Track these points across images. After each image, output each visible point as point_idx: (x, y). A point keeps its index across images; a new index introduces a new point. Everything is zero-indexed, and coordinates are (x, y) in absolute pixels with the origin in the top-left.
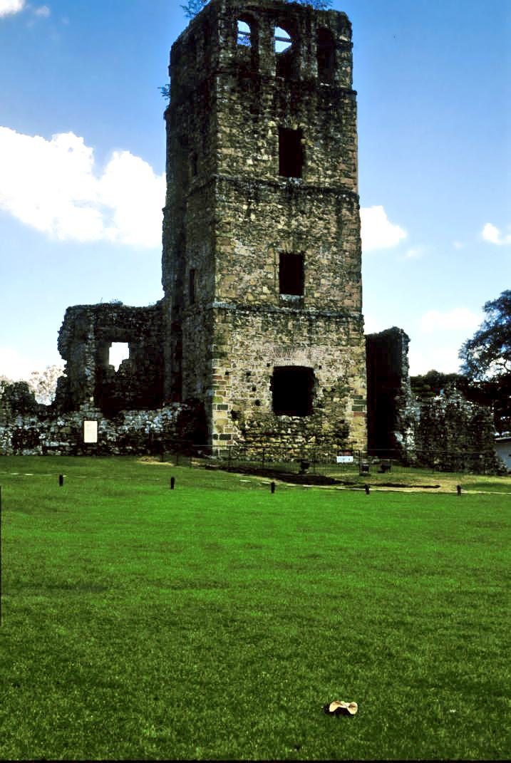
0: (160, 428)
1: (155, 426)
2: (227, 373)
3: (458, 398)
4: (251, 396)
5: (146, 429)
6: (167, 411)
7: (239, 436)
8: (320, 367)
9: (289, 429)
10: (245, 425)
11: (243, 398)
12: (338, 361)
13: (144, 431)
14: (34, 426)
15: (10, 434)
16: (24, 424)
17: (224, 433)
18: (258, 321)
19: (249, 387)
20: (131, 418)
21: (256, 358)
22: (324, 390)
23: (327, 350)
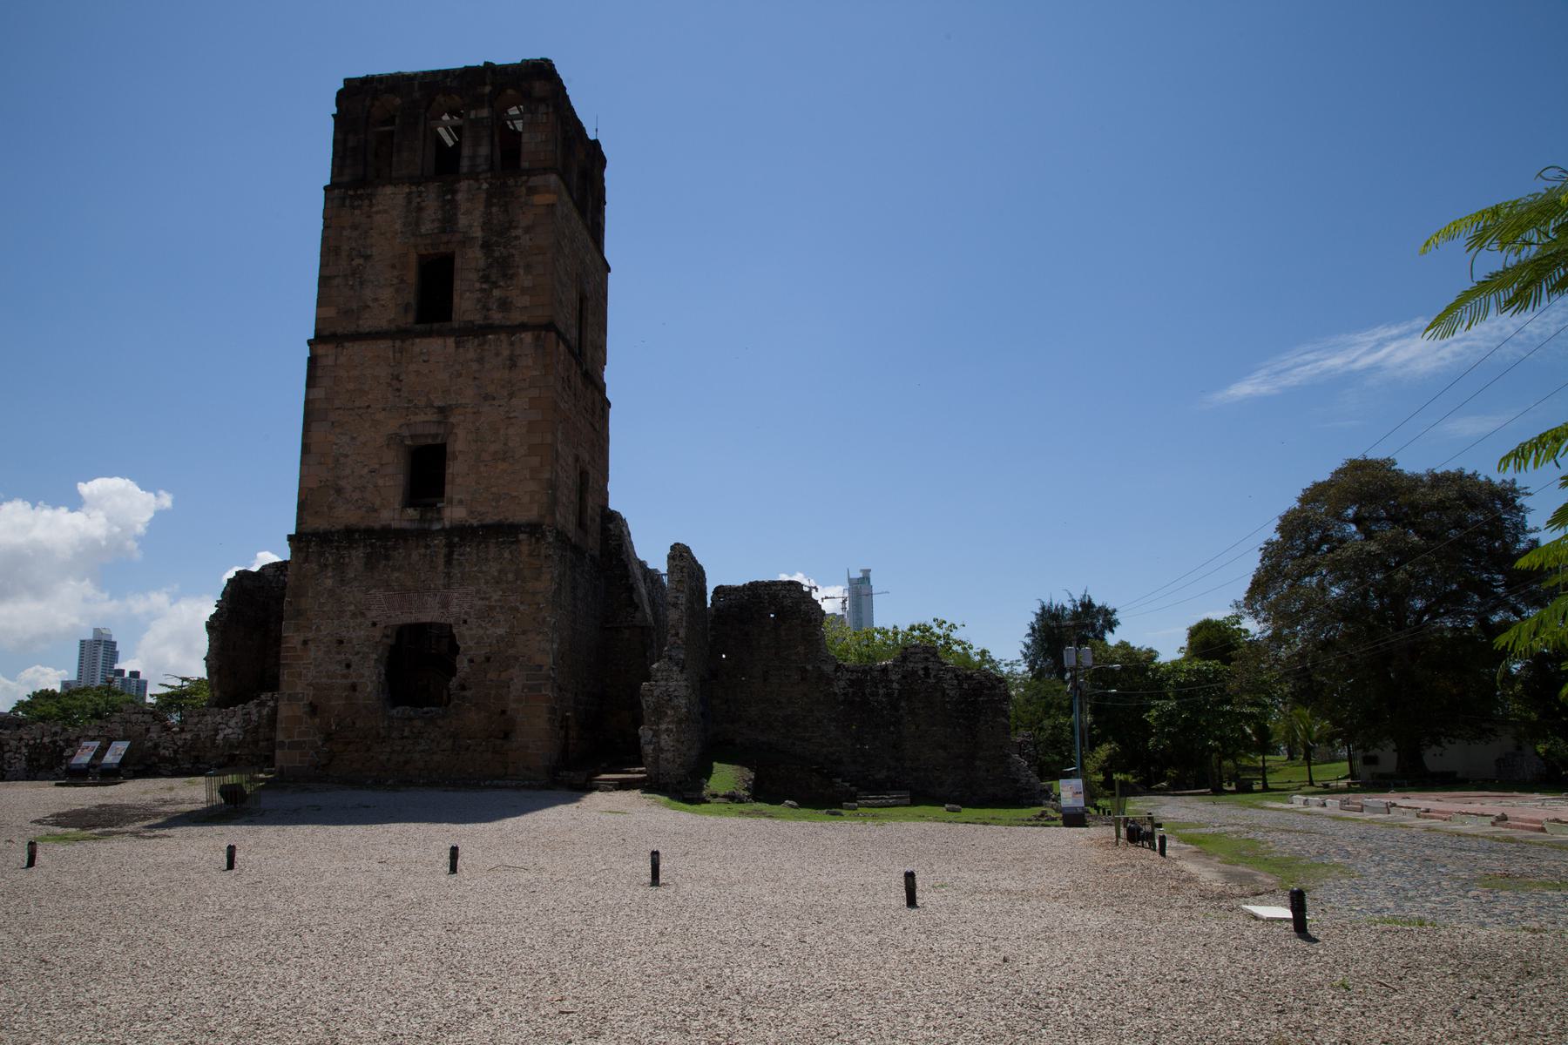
0: (239, 734)
1: (230, 731)
2: (305, 643)
3: (927, 659)
4: (345, 676)
5: (218, 738)
6: (251, 706)
7: (320, 743)
8: (465, 622)
9: (407, 729)
10: (331, 725)
11: (329, 681)
12: (498, 610)
13: (215, 739)
14: (58, 738)
15: (24, 750)
16: (43, 736)
17: (296, 739)
18: (357, 556)
19: (339, 662)
20: (196, 720)
21: (354, 615)
22: (471, 661)
23: (478, 592)
